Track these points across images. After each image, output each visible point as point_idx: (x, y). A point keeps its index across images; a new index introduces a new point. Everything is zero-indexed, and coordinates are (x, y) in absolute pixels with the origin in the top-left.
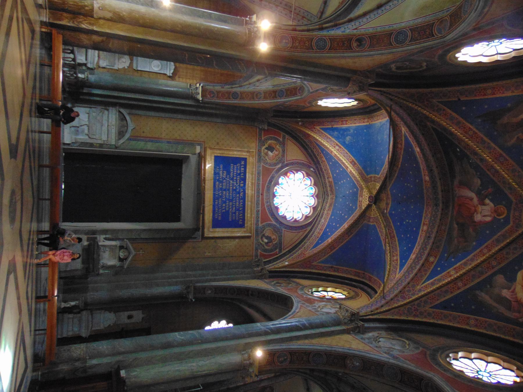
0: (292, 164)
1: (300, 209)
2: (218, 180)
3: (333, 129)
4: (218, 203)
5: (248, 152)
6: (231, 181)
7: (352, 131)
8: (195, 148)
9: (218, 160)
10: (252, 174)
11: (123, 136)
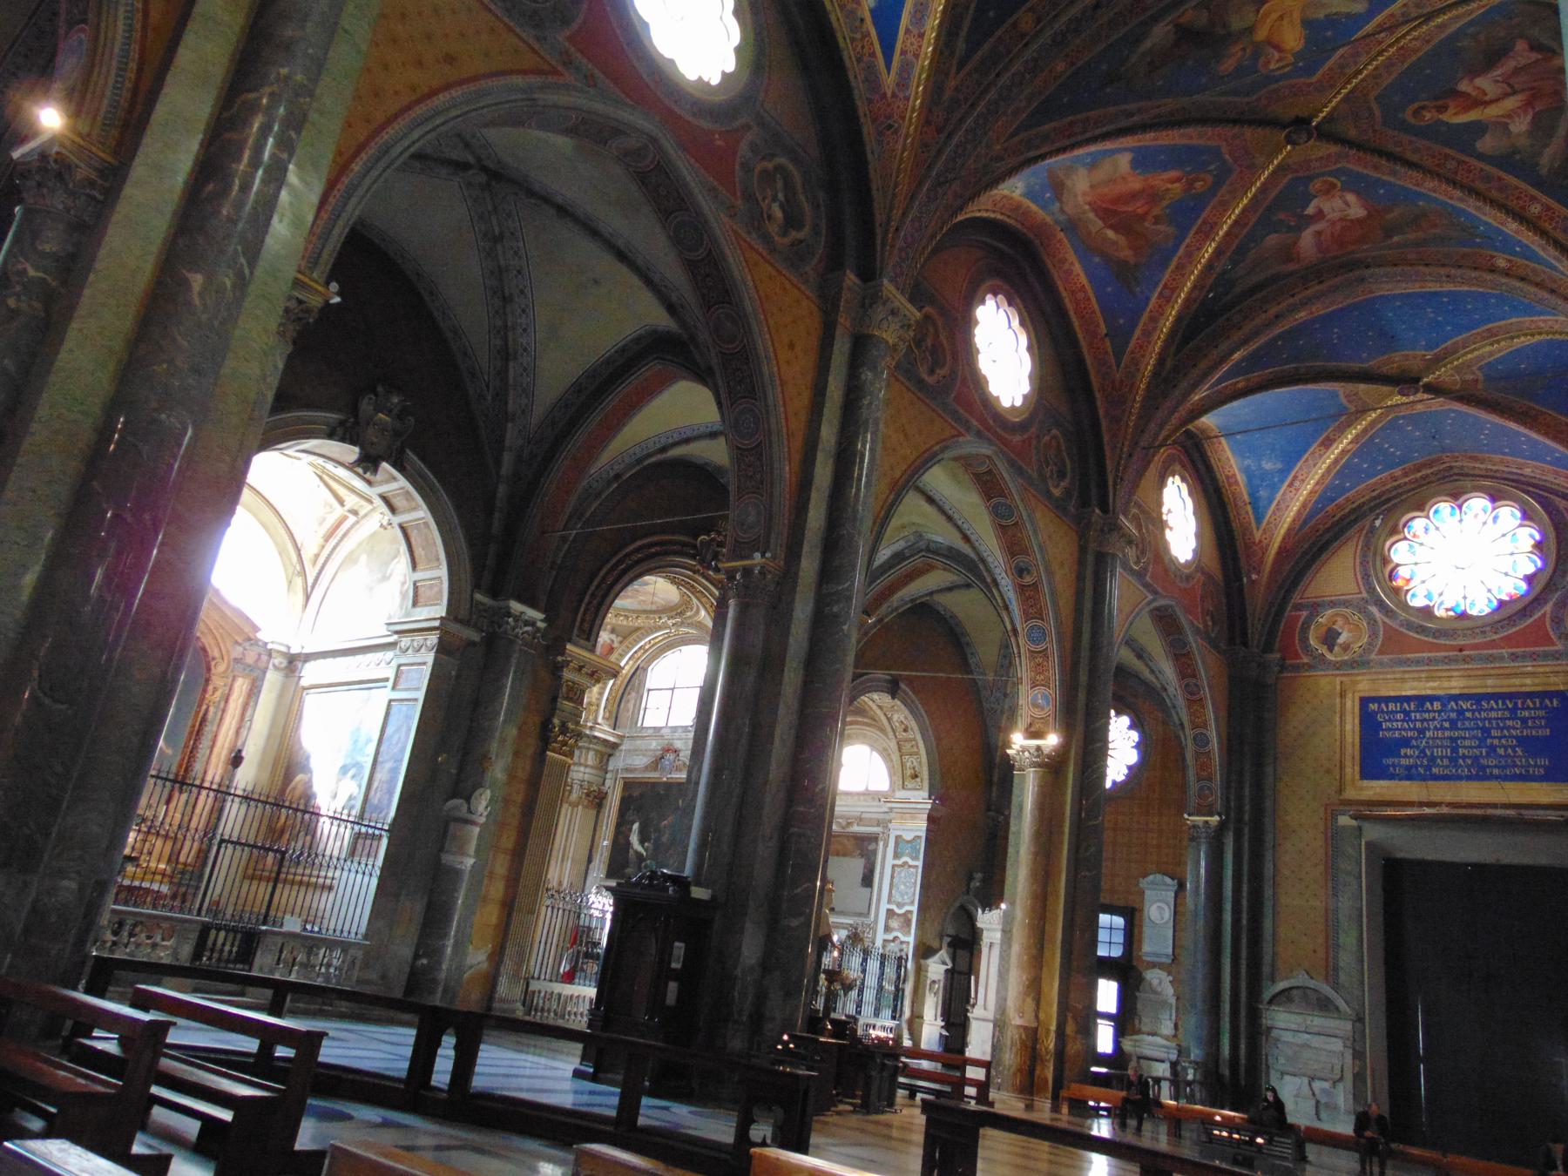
0: (1366, 577)
1: (1504, 535)
2: (1428, 768)
3: (1255, 501)
4: (1496, 766)
5: (1343, 695)
6: (1428, 734)
7: (1247, 462)
8: (1343, 827)
9: (1371, 769)
10: (1403, 680)
11: (1328, 999)
